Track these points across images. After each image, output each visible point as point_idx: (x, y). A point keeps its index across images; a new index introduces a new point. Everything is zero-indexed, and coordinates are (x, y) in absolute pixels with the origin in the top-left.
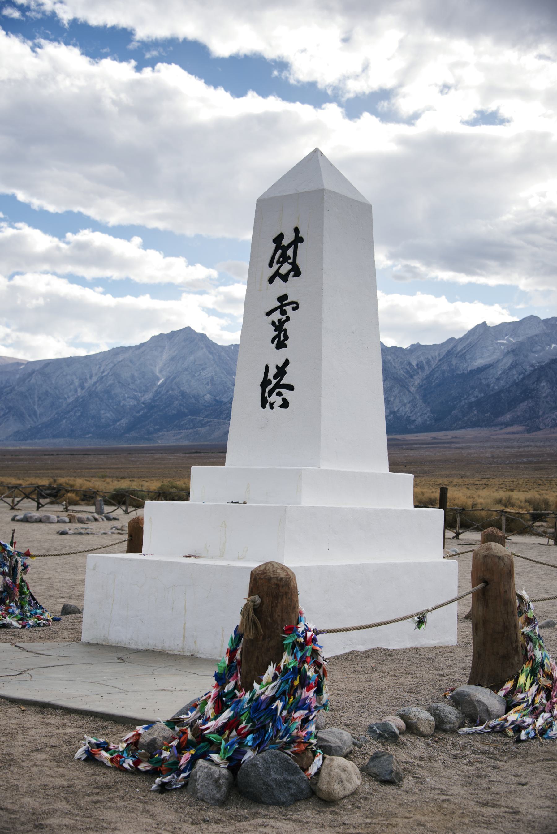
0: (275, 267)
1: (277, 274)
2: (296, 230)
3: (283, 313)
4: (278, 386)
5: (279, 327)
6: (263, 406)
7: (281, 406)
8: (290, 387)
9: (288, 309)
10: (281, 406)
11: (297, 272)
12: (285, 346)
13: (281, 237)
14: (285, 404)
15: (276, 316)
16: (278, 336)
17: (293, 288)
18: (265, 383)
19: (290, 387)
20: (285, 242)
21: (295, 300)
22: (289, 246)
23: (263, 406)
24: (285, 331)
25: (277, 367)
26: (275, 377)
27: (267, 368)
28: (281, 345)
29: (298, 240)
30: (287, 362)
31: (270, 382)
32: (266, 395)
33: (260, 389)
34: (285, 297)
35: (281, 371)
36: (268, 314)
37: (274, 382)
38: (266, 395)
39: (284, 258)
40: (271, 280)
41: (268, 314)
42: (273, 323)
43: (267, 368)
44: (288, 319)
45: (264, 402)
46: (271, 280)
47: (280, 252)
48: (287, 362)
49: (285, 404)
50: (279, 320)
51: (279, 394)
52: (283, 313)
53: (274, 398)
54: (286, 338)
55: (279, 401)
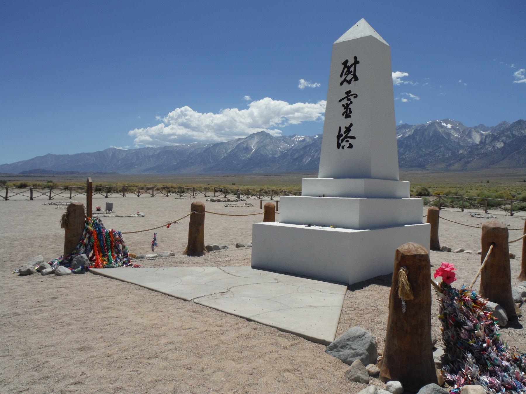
0: (344, 77)
1: (345, 80)
2: (355, 58)
3: (349, 100)
4: (346, 137)
7: (348, 147)
8: (353, 138)
9: (352, 98)
10: (348, 147)
11: (356, 78)
12: (350, 117)
14: (351, 146)
15: (345, 102)
16: (346, 112)
17: (353, 87)
19: (353, 138)
20: (349, 64)
22: (352, 66)
24: (350, 109)
25: (346, 127)
26: (345, 133)
27: (340, 128)
28: (348, 116)
29: (356, 62)
30: (351, 125)
31: (342, 135)
32: (340, 142)
34: (350, 92)
35: (348, 130)
36: (340, 101)
37: (344, 135)
38: (340, 142)
39: (349, 72)
40: (342, 84)
41: (340, 101)
42: (343, 105)
43: (340, 128)
44: (351, 103)
45: (339, 146)
46: (342, 84)
47: (346, 69)
48: (351, 125)
49: (351, 146)
50: (347, 104)
51: (347, 141)
54: (351, 112)
55: (347, 145)
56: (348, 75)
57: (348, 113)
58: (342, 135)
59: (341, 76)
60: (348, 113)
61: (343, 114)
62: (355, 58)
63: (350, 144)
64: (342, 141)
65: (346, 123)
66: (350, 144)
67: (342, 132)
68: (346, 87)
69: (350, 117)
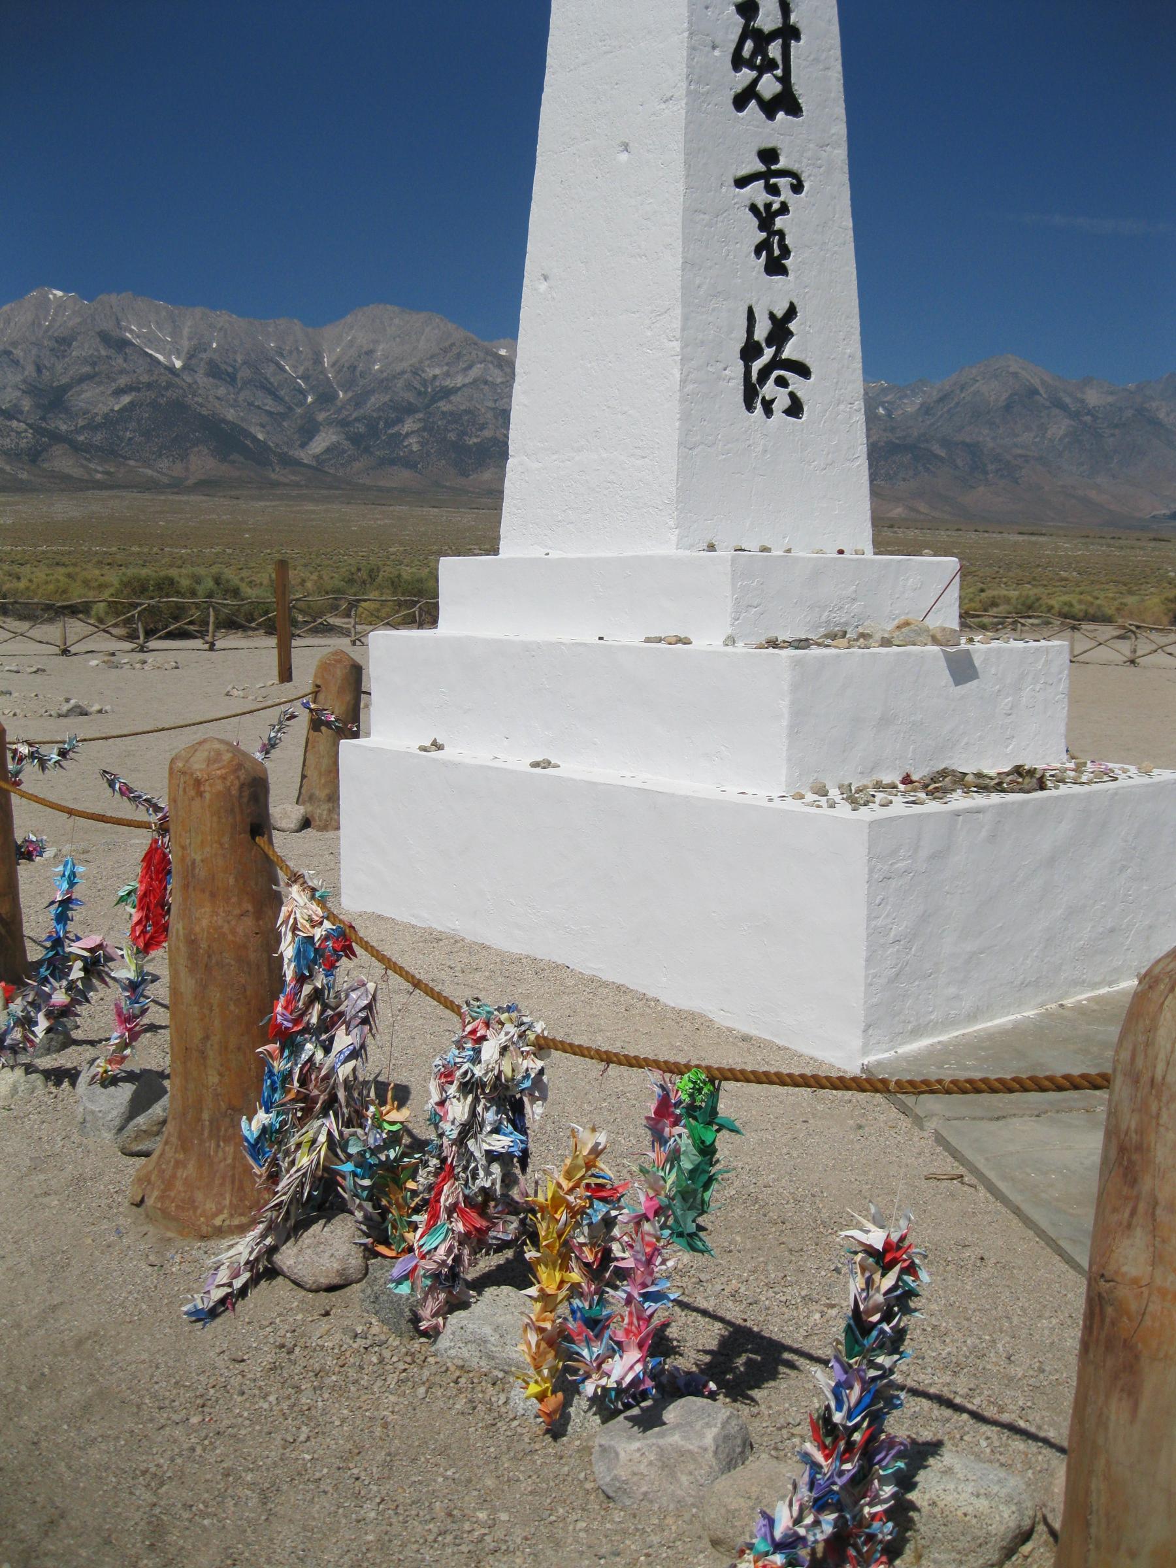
3: (774, 190)
5: (765, 218)
6: (750, 407)
8: (803, 370)
9: (783, 183)
12: (784, 271)
14: (795, 409)
18: (750, 351)
19: (803, 370)
21: (795, 167)
22: (773, 35)
23: (750, 407)
24: (781, 234)
25: (772, 316)
26: (770, 341)
27: (751, 312)
30: (792, 312)
33: (740, 365)
35: (780, 331)
36: (741, 182)
37: (769, 353)
40: (740, 102)
41: (741, 182)
42: (753, 208)
43: (751, 312)
44: (784, 209)
45: (750, 395)
46: (740, 102)
48: (792, 312)
50: (768, 206)
51: (782, 382)
52: (774, 190)
53: (769, 389)
54: (786, 252)
55: (782, 401)
56: (761, 71)
57: (777, 252)
58: (759, 352)
60: (777, 252)
61: (758, 251)
63: (792, 395)
64: (764, 374)
65: (773, 295)
66: (792, 395)
69: (784, 271)
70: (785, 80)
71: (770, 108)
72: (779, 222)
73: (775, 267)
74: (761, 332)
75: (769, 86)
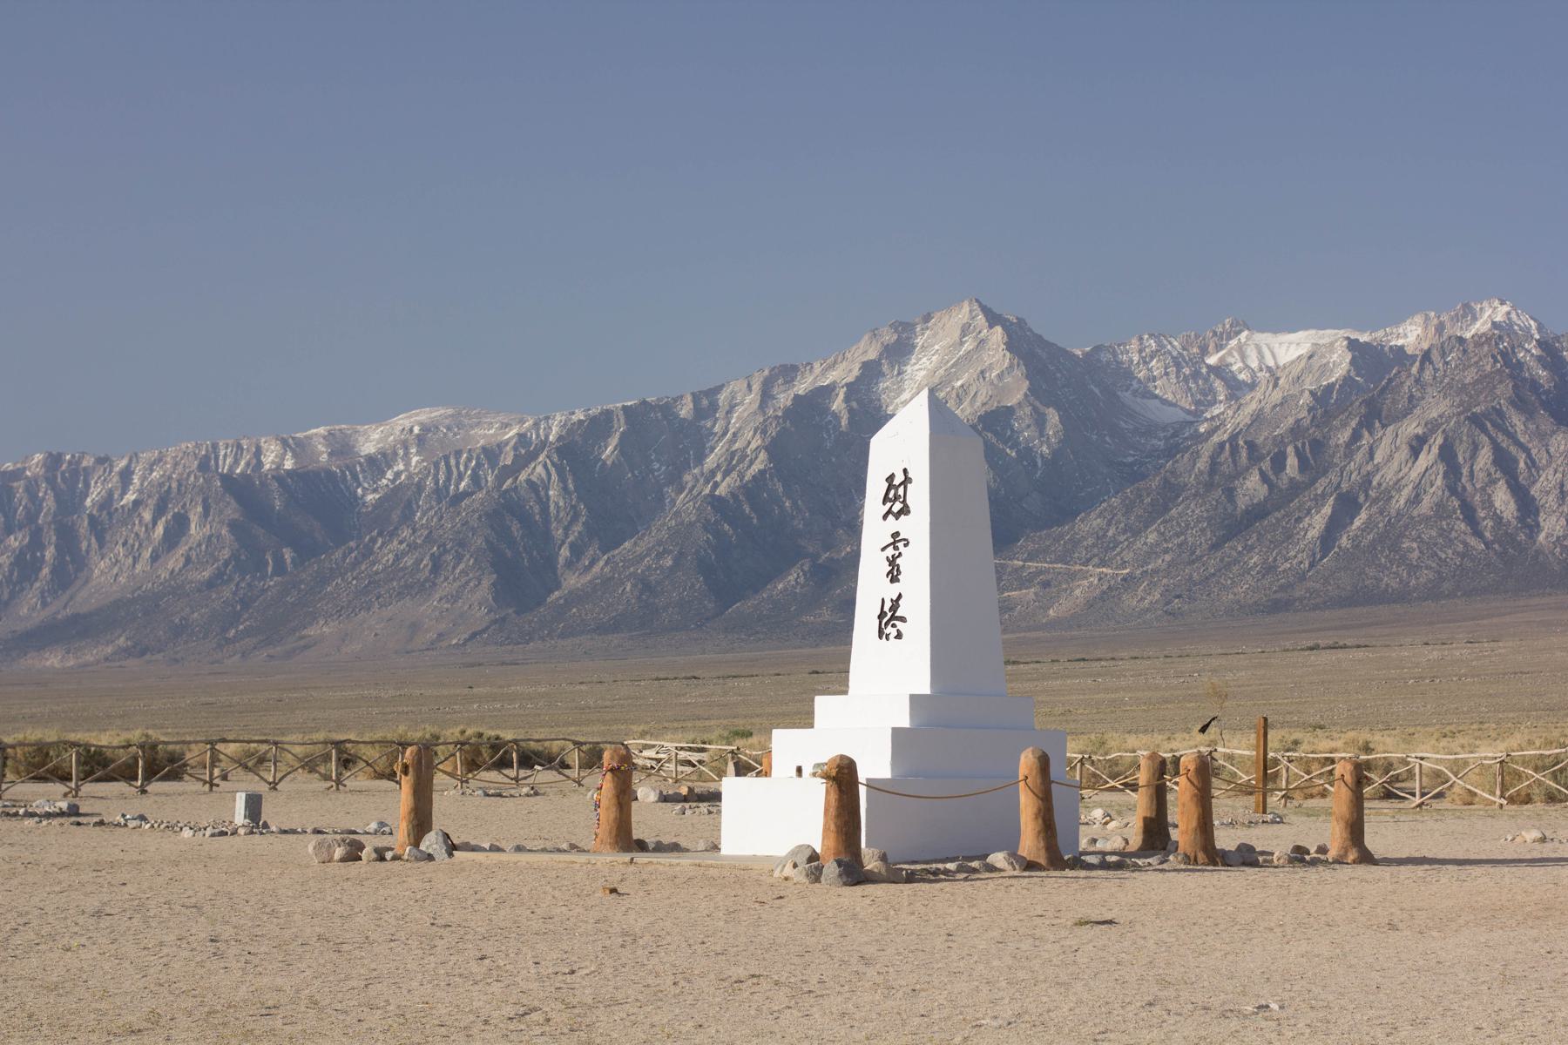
2: (905, 471)
3: (896, 548)
5: (892, 562)
8: (903, 619)
9: (900, 545)
11: (905, 510)
13: (891, 478)
14: (899, 636)
15: (890, 552)
16: (891, 572)
18: (882, 615)
19: (903, 619)
20: (897, 482)
28: (894, 580)
29: (907, 480)
34: (897, 534)
35: (895, 604)
36: (883, 549)
39: (896, 498)
40: (885, 517)
41: (883, 549)
45: (881, 633)
46: (885, 517)
49: (899, 636)
52: (896, 548)
53: (889, 630)
55: (893, 632)
59: (886, 500)
62: (905, 471)
65: (891, 592)
67: (886, 609)
68: (892, 524)
70: (904, 502)
71: (897, 516)
72: (898, 561)
73: (894, 580)
74: (888, 605)
75: (897, 506)
